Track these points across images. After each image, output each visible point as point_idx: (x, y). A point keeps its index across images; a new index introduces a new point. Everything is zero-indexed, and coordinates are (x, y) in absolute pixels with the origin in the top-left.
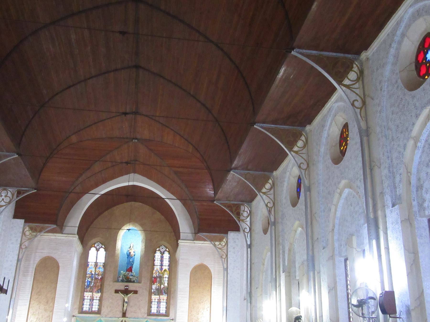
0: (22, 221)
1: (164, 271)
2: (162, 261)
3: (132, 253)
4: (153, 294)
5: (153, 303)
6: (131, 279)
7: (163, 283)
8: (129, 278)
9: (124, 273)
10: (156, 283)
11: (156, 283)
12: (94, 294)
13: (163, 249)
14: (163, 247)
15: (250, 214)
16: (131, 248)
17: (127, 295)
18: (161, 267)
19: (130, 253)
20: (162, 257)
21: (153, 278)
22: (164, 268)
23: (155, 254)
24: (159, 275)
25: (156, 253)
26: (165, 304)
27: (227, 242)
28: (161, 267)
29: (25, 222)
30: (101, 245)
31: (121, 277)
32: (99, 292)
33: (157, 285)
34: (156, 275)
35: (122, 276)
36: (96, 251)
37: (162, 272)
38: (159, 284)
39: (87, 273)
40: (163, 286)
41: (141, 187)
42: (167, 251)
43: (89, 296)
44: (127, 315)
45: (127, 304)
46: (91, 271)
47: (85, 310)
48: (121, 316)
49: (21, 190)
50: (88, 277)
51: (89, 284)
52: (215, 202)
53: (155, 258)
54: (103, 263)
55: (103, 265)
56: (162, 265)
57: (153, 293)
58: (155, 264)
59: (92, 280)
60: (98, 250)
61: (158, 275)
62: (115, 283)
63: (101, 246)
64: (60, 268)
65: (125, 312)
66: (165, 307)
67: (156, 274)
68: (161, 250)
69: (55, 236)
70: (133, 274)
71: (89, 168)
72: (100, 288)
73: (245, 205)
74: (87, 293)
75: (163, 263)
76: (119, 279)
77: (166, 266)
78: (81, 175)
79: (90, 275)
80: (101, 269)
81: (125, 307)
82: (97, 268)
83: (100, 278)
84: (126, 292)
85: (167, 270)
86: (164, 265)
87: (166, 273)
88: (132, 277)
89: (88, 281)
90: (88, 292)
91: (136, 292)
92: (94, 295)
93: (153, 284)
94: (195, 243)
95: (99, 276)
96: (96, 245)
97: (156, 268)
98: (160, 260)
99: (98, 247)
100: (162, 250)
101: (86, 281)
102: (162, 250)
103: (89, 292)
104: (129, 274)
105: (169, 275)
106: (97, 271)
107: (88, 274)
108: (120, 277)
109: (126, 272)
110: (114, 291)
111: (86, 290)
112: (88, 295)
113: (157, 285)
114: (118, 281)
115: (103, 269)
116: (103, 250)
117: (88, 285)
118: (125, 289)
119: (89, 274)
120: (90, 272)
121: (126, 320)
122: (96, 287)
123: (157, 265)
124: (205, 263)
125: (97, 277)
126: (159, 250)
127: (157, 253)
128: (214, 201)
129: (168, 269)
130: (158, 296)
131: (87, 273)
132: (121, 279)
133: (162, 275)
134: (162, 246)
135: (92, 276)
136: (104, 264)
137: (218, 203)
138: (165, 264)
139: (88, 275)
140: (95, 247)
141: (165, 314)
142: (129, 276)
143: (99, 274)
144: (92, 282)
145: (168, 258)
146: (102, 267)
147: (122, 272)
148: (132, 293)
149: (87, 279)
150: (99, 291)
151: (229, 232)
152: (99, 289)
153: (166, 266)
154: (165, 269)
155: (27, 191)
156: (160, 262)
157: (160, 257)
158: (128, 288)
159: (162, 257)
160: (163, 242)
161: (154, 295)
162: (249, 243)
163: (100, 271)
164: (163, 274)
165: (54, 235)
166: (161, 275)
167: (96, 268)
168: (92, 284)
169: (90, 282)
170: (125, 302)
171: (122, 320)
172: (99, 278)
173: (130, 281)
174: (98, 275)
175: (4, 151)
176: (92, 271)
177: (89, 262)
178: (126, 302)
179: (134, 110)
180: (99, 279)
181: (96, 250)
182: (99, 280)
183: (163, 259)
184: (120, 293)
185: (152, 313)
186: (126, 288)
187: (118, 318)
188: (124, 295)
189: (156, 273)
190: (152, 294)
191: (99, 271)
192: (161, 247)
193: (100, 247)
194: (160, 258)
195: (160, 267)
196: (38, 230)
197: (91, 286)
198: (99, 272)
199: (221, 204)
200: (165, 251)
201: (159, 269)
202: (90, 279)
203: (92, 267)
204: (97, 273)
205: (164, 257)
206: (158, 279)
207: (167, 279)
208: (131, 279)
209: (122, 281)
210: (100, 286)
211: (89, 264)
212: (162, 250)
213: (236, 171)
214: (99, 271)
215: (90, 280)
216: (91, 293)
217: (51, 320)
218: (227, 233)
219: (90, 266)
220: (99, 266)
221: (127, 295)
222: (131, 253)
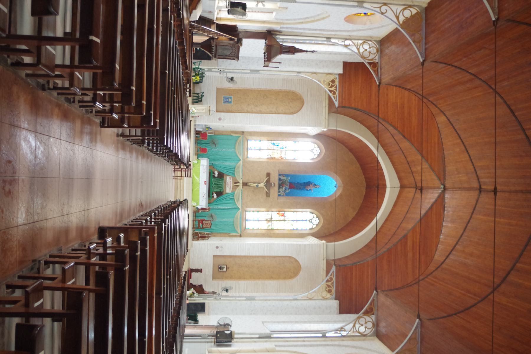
0: (341, 72)
3: (309, 188)
6: (281, 189)
8: (282, 186)
9: (288, 181)
15: (362, 336)
16: (315, 186)
17: (265, 186)
19: (310, 185)
27: (327, 299)
29: (339, 75)
31: (284, 178)
35: (284, 179)
36: (310, 150)
41: (385, 194)
44: (245, 187)
45: (256, 187)
48: (244, 182)
49: (377, 68)
52: (375, 291)
62: (277, 172)
64: (292, 115)
65: (248, 185)
69: (326, 107)
70: (287, 190)
71: (404, 137)
73: (372, 330)
76: (282, 176)
78: (396, 128)
79: (284, 146)
81: (253, 185)
84: (268, 184)
88: (284, 188)
91: (268, 195)
94: (323, 260)
104: (287, 185)
108: (284, 177)
109: (289, 183)
110: (268, 172)
114: (280, 175)
118: (272, 183)
121: (239, 187)
124: (301, 272)
126: (314, 217)
128: (377, 291)
132: (282, 178)
137: (374, 296)
142: (285, 186)
147: (289, 178)
148: (267, 191)
151: (338, 301)
155: (377, 75)
158: (273, 186)
160: (322, 221)
162: (327, 335)
165: (326, 105)
170: (258, 185)
171: (240, 182)
173: (279, 188)
175: (427, 46)
178: (258, 186)
179: (482, 187)
184: (268, 178)
186: (273, 184)
187: (242, 179)
188: (265, 182)
196: (332, 89)
199: (373, 300)
206: (282, 218)
208: (282, 188)
209: (280, 179)
213: (419, 326)
217: (239, 111)
218: (336, 299)
221: (265, 186)
222: (309, 187)
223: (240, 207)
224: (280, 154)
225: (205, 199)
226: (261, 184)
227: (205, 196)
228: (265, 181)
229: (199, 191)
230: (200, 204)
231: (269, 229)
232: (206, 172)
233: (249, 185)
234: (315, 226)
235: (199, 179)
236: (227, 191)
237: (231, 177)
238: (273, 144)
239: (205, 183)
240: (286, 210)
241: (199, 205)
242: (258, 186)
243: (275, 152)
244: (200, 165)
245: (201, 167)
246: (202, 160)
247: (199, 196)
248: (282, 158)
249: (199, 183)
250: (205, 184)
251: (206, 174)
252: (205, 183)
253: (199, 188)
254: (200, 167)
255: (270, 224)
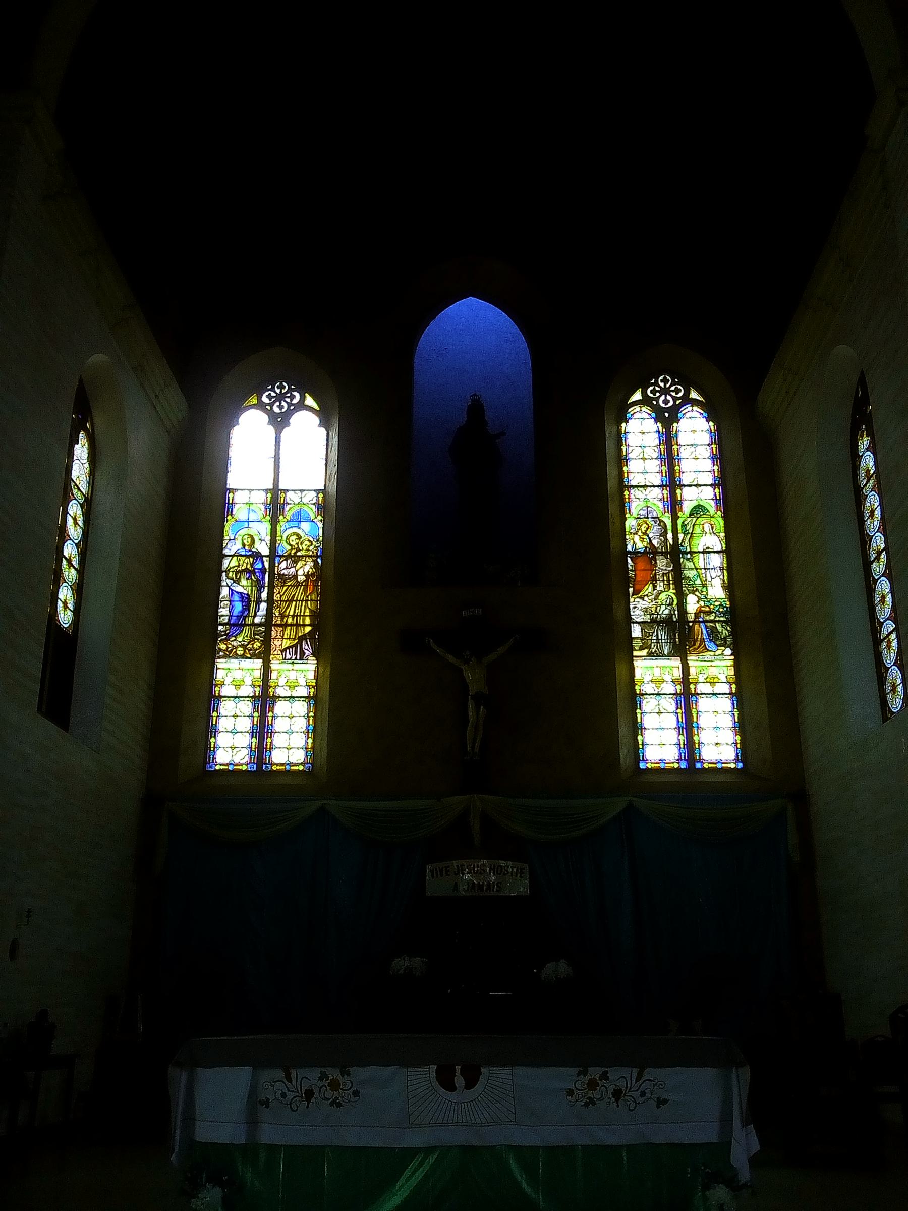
1: (691, 514)
2: (670, 458)
4: (641, 649)
5: (648, 705)
7: (698, 582)
10: (654, 588)
11: (654, 588)
12: (275, 665)
13: (665, 391)
14: (665, 381)
18: (673, 494)
20: (668, 440)
21: (629, 560)
22: (689, 497)
23: (624, 425)
24: (666, 540)
25: (627, 422)
26: (726, 704)
28: (673, 494)
30: (297, 395)
32: (307, 653)
33: (656, 598)
34: (642, 540)
36: (271, 430)
37: (679, 522)
38: (672, 591)
39: (226, 552)
40: (700, 599)
42: (694, 402)
43: (248, 681)
46: (252, 537)
47: (227, 765)
50: (230, 575)
51: (242, 612)
53: (624, 448)
54: (318, 491)
55: (317, 504)
56: (672, 483)
57: (637, 644)
58: (631, 476)
59: (260, 586)
60: (280, 422)
61: (655, 542)
63: (296, 400)
66: (731, 724)
67: (645, 533)
68: (657, 399)
72: (308, 629)
74: (234, 663)
75: (677, 468)
77: (698, 486)
79: (246, 563)
80: (305, 526)
82: (281, 518)
83: (307, 576)
85: (711, 506)
86: (685, 481)
87: (707, 528)
89: (232, 592)
90: (236, 656)
92: (274, 675)
93: (636, 593)
95: (300, 564)
96: (269, 397)
97: (643, 504)
98: (656, 455)
99: (281, 407)
100: (663, 397)
101: (225, 592)
102: (666, 402)
103: (243, 657)
105: (727, 537)
106: (284, 538)
107: (233, 556)
111: (223, 647)
112: (238, 675)
113: (656, 598)
115: (321, 525)
116: (316, 420)
117: (238, 617)
119: (237, 555)
120: (244, 545)
122: (284, 631)
123: (645, 486)
125: (285, 572)
126: (645, 401)
127: (637, 415)
129: (713, 503)
130: (676, 662)
131: (226, 552)
133: (681, 536)
134: (661, 378)
135: (260, 566)
136: (321, 495)
138: (693, 476)
139: (234, 562)
140: (261, 406)
141: (733, 766)
143: (299, 554)
144: (259, 601)
145: (706, 439)
146: (311, 511)
149: (224, 584)
150: (304, 646)
152: (301, 639)
153: (698, 486)
154: (695, 503)
156: (658, 469)
157: (653, 439)
159: (668, 440)
161: (650, 655)
163: (302, 534)
164: (685, 534)
166: (675, 538)
167: (274, 522)
168: (257, 609)
169: (245, 599)
172: (300, 572)
174: (295, 558)
176: (256, 539)
177: (233, 491)
178: (479, 699)
180: (301, 578)
181: (270, 423)
182: (298, 584)
183: (675, 447)
185: (649, 766)
189: (643, 529)
190: (632, 649)
191: (294, 537)
192: (656, 384)
193: (289, 404)
194: (657, 442)
195: (665, 492)
197: (257, 620)
198: (293, 543)
200: (682, 405)
201: (660, 504)
202: (244, 582)
203: (253, 517)
204: (284, 548)
205: (682, 439)
206: (662, 563)
207: (717, 560)
210: (308, 621)
211: (236, 501)
212: (666, 402)
214: (294, 534)
215: (244, 586)
216: (258, 663)
219: (240, 512)
220: (297, 508)
223: (619, 804)
224: (298, 584)
225: (650, 1073)
226: (469, 676)
227: (614, 1073)
228: (450, 658)
229: (551, 1150)
230: (709, 1134)
231: (733, 633)
232: (334, 1073)
233: (477, 750)
234: (694, 395)
235: (410, 1153)
236: (522, 887)
237: (429, 867)
238: (237, 624)
239: (459, 1081)
240: (614, 543)
241: (724, 1147)
242: (479, 699)
243: (282, 616)
244: (250, 1150)
245: (269, 1134)
246: (189, 1119)
247: (618, 1148)
248: (318, 576)
249: (466, 1149)
250: (470, 1084)
251: (360, 1073)
252: (459, 1081)
253: (518, 1150)
254: (272, 1149)
255: (701, 630)
